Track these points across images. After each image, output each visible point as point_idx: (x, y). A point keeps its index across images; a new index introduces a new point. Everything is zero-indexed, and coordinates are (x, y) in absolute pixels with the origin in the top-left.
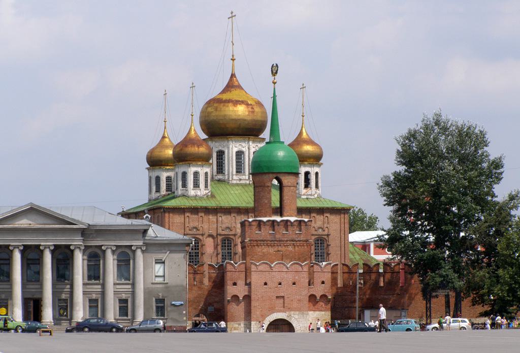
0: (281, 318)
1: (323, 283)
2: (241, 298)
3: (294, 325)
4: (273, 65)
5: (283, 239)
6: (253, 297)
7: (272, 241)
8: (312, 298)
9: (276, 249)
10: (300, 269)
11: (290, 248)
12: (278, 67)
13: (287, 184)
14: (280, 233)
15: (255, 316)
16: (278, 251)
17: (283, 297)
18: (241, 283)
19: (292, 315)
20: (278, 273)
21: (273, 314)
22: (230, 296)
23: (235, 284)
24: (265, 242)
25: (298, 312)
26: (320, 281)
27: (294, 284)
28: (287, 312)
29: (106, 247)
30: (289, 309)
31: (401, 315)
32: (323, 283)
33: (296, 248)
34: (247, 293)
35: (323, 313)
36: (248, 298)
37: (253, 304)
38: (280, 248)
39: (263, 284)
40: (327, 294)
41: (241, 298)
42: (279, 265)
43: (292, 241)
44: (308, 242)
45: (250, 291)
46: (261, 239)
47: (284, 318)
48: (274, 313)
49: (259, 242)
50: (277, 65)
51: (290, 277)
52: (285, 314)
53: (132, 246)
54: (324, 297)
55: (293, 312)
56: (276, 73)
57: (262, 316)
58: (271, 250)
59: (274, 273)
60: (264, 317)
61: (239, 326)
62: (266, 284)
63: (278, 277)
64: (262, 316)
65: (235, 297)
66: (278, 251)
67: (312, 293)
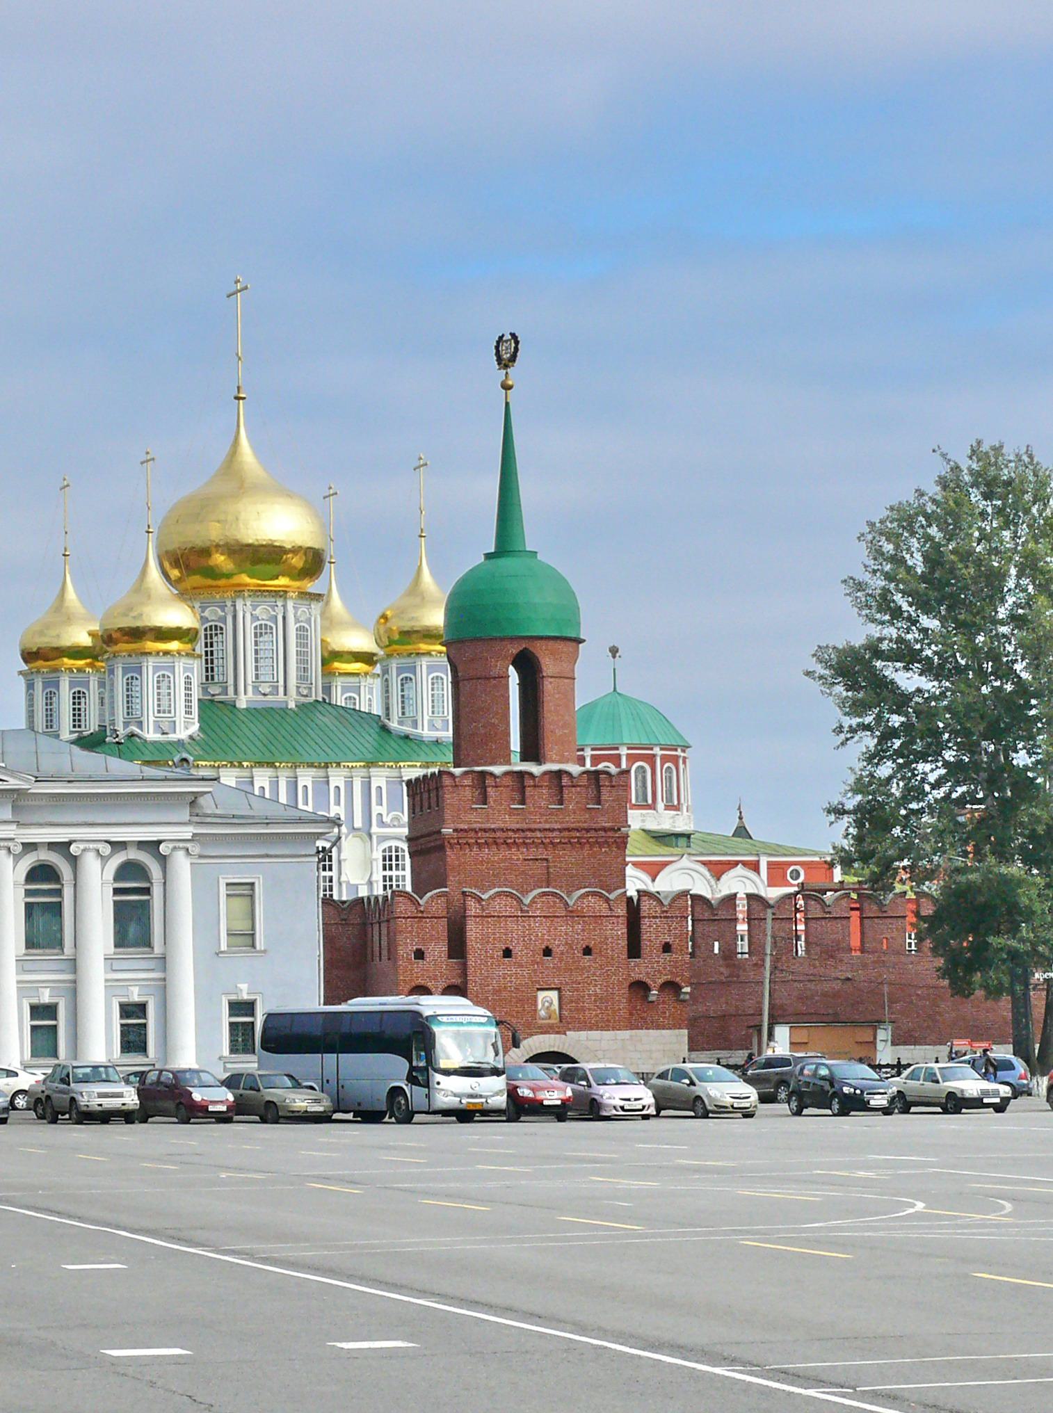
4: (501, 338)
8: (640, 988)
12: (517, 343)
18: (438, 950)
26: (658, 943)
27: (587, 951)
29: (82, 846)
31: (875, 1038)
32: (667, 948)
34: (457, 981)
42: (544, 899)
50: (513, 336)
51: (575, 933)
53: (159, 842)
54: (672, 987)
56: (513, 358)
62: (507, 953)
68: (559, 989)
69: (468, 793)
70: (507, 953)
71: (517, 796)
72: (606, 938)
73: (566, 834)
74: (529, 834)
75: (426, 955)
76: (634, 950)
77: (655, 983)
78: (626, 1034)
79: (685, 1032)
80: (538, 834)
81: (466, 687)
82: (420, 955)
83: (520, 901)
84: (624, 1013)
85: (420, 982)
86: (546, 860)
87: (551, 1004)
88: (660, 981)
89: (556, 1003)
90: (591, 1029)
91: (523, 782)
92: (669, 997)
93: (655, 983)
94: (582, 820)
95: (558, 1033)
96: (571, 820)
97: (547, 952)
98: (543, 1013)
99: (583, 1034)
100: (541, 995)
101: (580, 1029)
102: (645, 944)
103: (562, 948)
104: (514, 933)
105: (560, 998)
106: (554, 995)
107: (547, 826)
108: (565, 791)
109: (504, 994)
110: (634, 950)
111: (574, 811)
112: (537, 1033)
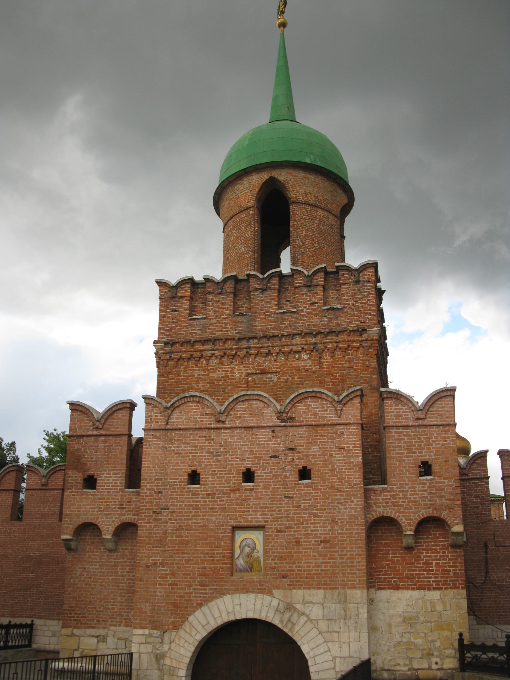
0: (251, 615)
1: (426, 468)
3: (305, 649)
5: (277, 333)
7: (240, 339)
9: (254, 364)
10: (329, 414)
11: (305, 360)
13: (303, 199)
14: (267, 313)
15: (146, 607)
16: (263, 372)
18: (112, 477)
19: (299, 606)
20: (245, 432)
21: (219, 601)
23: (90, 482)
24: (219, 345)
25: (318, 595)
30: (284, 577)
32: (426, 468)
33: (326, 358)
35: (435, 595)
38: (268, 363)
40: (444, 514)
42: (246, 405)
43: (309, 334)
44: (365, 336)
46: (207, 336)
47: (263, 617)
48: (222, 593)
52: (268, 598)
54: (429, 524)
55: (300, 592)
57: (176, 606)
58: (238, 370)
59: (225, 435)
60: (180, 612)
61: (102, 646)
62: (194, 478)
63: (241, 448)
64: (176, 606)
65: (88, 528)
66: (263, 372)
67: (379, 511)
68: (261, 528)
70: (194, 478)
75: (99, 482)
77: (408, 522)
79: (464, 592)
82: (90, 482)
84: (361, 563)
87: (254, 548)
89: (260, 547)
90: (309, 587)
93: (408, 522)
98: (241, 562)
100: (240, 536)
105: (266, 541)
106: (257, 537)
109: (185, 533)
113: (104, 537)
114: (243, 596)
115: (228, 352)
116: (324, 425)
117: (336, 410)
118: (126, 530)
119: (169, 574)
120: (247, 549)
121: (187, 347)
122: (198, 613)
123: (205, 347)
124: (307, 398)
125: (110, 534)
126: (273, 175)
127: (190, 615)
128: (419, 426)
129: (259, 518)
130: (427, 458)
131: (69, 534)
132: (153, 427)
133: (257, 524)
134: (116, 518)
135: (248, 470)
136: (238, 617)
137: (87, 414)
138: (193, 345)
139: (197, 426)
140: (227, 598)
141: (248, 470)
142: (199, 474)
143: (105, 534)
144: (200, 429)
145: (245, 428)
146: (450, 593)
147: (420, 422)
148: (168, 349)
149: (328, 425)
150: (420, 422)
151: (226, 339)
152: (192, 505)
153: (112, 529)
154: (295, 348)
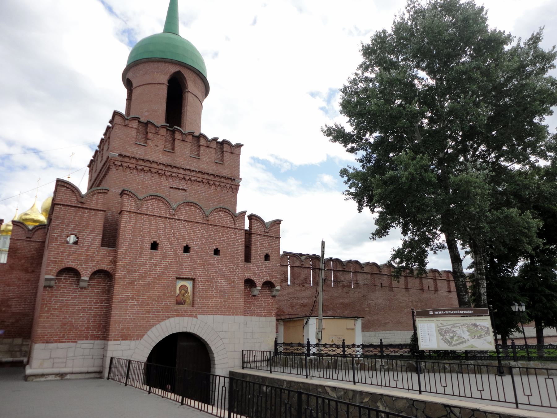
2: (85, 278)
6: (120, 272)
8: (250, 283)
17: (193, 279)
22: (55, 270)
27: (217, 252)
28: (199, 316)
34: (106, 267)
36: (105, 276)
37: (119, 291)
39: (149, 246)
41: (85, 278)
42: (188, 208)
44: (233, 183)
45: (114, 262)
49: (140, 162)
54: (269, 285)
62: (154, 246)
68: (193, 279)
69: (134, 133)
70: (154, 246)
71: (169, 145)
72: (230, 245)
73: (200, 175)
74: (175, 170)
76: (248, 259)
77: (259, 283)
78: (241, 318)
80: (181, 171)
81: (135, 93)
83: (168, 204)
85: (71, 264)
86: (185, 190)
87: (187, 292)
88: (263, 280)
90: (216, 314)
91: (174, 136)
92: (266, 293)
93: (259, 283)
94: (212, 169)
95: (191, 316)
96: (204, 167)
97: (187, 249)
99: (210, 318)
100: (180, 283)
101: (208, 313)
102: (253, 252)
103: (198, 247)
104: (160, 231)
105: (194, 287)
107: (188, 168)
108: (202, 148)
110: (248, 259)
111: (207, 162)
112: (173, 316)
113: (82, 278)
114: (181, 318)
115: (160, 172)
116: (227, 227)
117: (234, 220)
118: (105, 276)
119: (136, 305)
120: (183, 291)
121: (134, 161)
122: (154, 329)
123: (145, 164)
124: (220, 211)
125: (87, 277)
126: (182, 71)
127: (148, 330)
128: (266, 236)
129: (191, 275)
130: (267, 252)
131: (53, 275)
132: (128, 210)
133: (191, 277)
134: (93, 266)
135: (187, 245)
136: (178, 331)
137: (72, 191)
138: (137, 161)
139: (158, 215)
140: (172, 320)
141: (187, 245)
142: (158, 244)
143: (83, 276)
144: (160, 217)
145: (186, 221)
146: (269, 319)
147: (266, 234)
148: (120, 159)
149: (230, 228)
150: (266, 234)
151: (160, 163)
152: (153, 263)
153: (89, 273)
154: (198, 179)
